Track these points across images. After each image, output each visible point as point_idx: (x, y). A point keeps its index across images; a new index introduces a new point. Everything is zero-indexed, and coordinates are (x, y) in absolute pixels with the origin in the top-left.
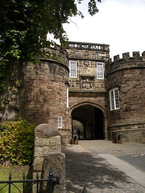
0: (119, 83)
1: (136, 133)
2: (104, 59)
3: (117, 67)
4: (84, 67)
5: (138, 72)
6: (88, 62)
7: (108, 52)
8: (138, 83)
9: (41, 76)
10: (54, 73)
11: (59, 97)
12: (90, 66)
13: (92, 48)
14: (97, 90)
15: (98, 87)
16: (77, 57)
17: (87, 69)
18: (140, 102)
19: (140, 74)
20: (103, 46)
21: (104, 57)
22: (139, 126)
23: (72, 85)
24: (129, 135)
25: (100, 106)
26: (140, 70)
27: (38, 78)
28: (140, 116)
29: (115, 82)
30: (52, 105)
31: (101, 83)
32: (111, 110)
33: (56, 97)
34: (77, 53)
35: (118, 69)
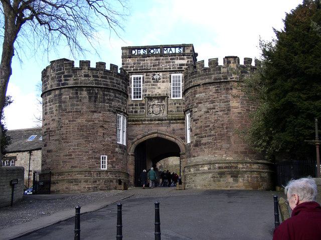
1: (205, 176)
8: (212, 105)
9: (79, 107)
10: (95, 102)
12: (162, 80)
13: (165, 52)
15: (171, 111)
16: (143, 69)
17: (156, 85)
18: (213, 132)
20: (184, 46)
21: (183, 65)
23: (134, 110)
33: (97, 131)
34: (143, 62)
35: (191, 86)
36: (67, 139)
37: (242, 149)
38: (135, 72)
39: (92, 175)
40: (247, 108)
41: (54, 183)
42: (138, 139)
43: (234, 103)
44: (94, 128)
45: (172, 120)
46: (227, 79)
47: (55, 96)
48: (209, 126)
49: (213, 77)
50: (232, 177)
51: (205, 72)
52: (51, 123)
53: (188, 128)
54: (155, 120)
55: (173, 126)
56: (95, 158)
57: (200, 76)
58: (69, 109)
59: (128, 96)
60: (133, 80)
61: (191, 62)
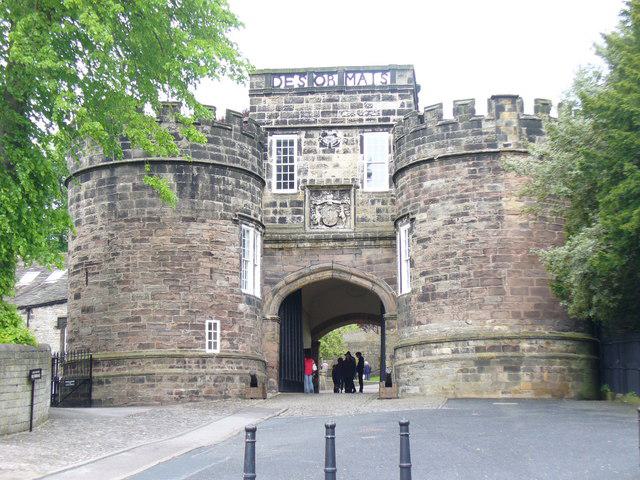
1: (445, 367)
2: (392, 117)
3: (409, 154)
5: (465, 172)
8: (460, 207)
10: (193, 197)
11: (211, 266)
12: (341, 147)
13: (350, 83)
14: (361, 231)
15: (363, 219)
16: (298, 122)
17: (329, 159)
18: (463, 269)
19: (470, 178)
20: (393, 70)
21: (391, 112)
22: (453, 346)
23: (278, 217)
24: (426, 374)
26: (471, 163)
27: (146, 216)
28: (461, 315)
31: (378, 205)
33: (198, 265)
34: (299, 106)
36: (127, 282)
37: (527, 306)
38: (280, 129)
39: (187, 364)
41: (100, 383)
42: (287, 284)
43: (511, 204)
44: (189, 258)
45: (365, 239)
46: (495, 146)
47: (101, 182)
48: (455, 254)
49: (464, 141)
50: (505, 369)
51: (444, 131)
52: (92, 244)
53: (403, 259)
54: (327, 240)
55: (367, 253)
56: (194, 326)
58: (133, 212)
59: (264, 183)
60: (275, 147)
61: (409, 105)
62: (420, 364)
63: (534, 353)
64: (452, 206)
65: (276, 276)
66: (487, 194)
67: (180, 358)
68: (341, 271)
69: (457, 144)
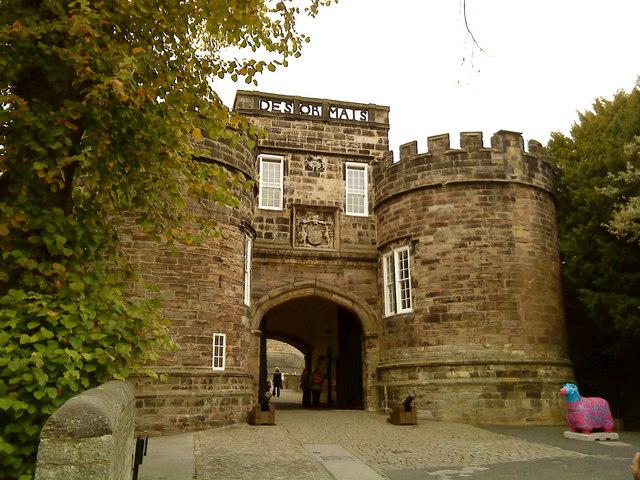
0: (413, 230)
1: (464, 392)
2: (371, 151)
3: (408, 180)
4: (307, 177)
5: (476, 199)
6: (320, 161)
7: (384, 129)
8: (472, 232)
11: (219, 272)
12: (325, 172)
13: (333, 116)
14: (346, 251)
15: (346, 241)
16: (284, 145)
17: (314, 182)
18: (477, 292)
19: (481, 204)
21: (371, 146)
23: (264, 232)
24: (440, 398)
25: (353, 301)
29: (401, 228)
30: (195, 296)
31: (359, 229)
32: (388, 313)
33: (208, 271)
35: (412, 187)
39: (193, 385)
40: (542, 244)
42: (271, 298)
43: (519, 232)
44: (199, 262)
45: (349, 259)
50: (528, 395)
54: (313, 257)
55: (349, 274)
56: (201, 340)
57: (440, 166)
62: (433, 387)
63: (549, 380)
64: (463, 230)
65: (262, 291)
66: (498, 221)
67: (185, 377)
68: (324, 289)
69: (467, 172)
